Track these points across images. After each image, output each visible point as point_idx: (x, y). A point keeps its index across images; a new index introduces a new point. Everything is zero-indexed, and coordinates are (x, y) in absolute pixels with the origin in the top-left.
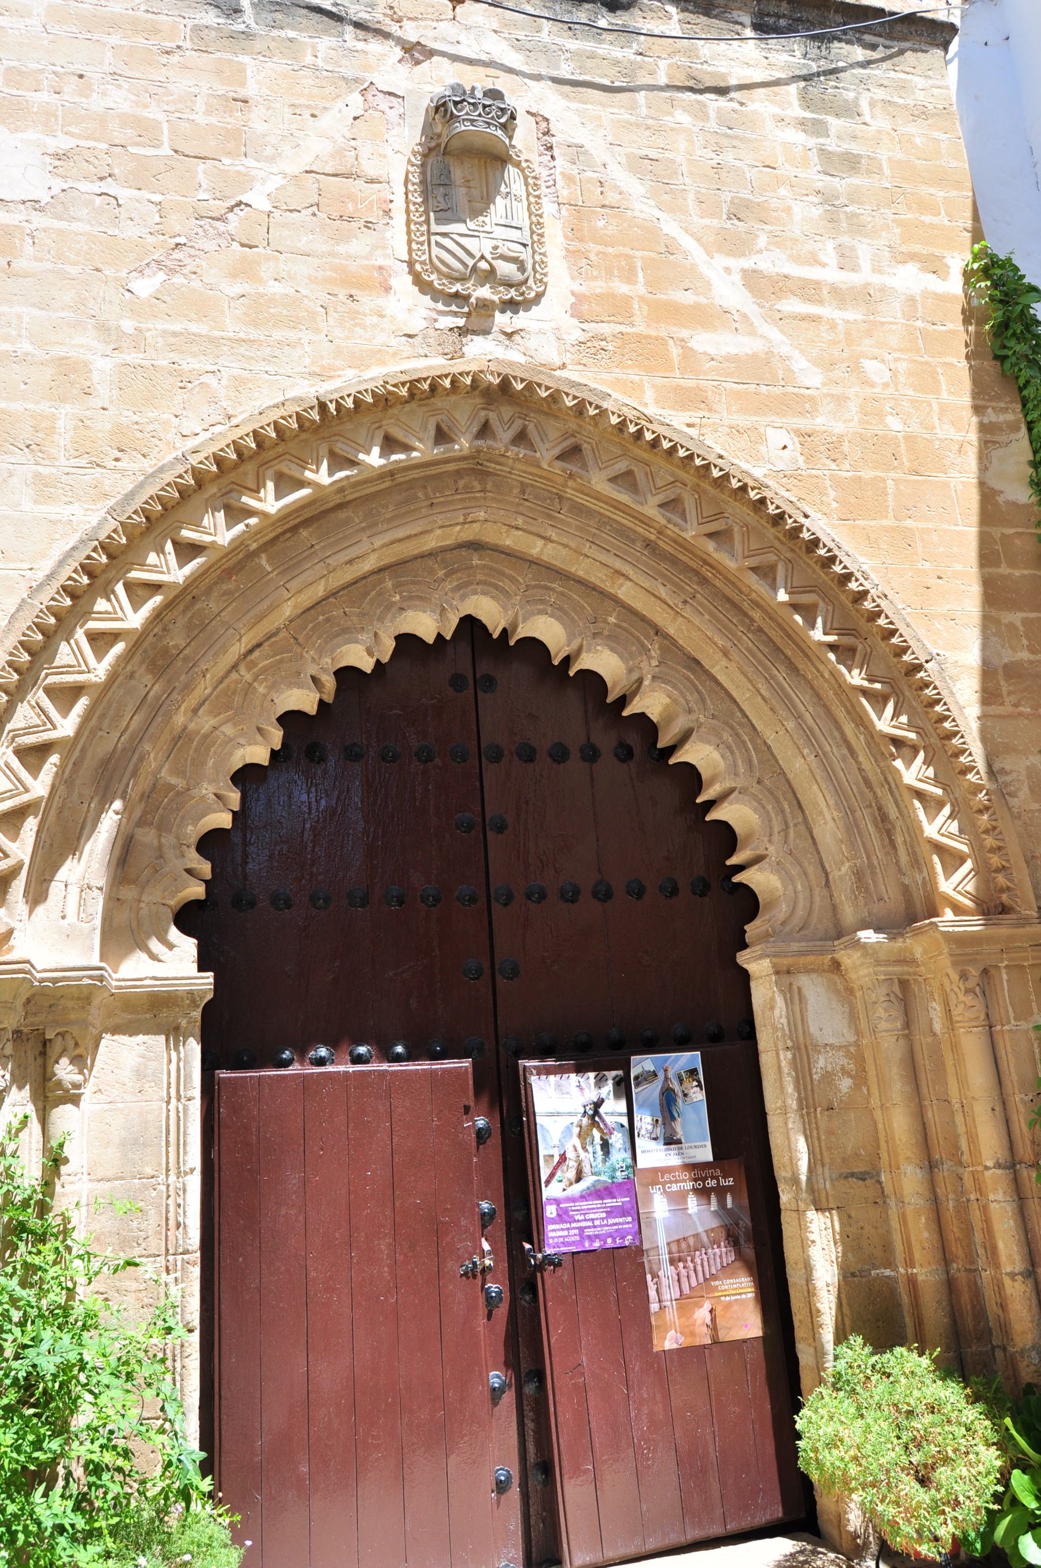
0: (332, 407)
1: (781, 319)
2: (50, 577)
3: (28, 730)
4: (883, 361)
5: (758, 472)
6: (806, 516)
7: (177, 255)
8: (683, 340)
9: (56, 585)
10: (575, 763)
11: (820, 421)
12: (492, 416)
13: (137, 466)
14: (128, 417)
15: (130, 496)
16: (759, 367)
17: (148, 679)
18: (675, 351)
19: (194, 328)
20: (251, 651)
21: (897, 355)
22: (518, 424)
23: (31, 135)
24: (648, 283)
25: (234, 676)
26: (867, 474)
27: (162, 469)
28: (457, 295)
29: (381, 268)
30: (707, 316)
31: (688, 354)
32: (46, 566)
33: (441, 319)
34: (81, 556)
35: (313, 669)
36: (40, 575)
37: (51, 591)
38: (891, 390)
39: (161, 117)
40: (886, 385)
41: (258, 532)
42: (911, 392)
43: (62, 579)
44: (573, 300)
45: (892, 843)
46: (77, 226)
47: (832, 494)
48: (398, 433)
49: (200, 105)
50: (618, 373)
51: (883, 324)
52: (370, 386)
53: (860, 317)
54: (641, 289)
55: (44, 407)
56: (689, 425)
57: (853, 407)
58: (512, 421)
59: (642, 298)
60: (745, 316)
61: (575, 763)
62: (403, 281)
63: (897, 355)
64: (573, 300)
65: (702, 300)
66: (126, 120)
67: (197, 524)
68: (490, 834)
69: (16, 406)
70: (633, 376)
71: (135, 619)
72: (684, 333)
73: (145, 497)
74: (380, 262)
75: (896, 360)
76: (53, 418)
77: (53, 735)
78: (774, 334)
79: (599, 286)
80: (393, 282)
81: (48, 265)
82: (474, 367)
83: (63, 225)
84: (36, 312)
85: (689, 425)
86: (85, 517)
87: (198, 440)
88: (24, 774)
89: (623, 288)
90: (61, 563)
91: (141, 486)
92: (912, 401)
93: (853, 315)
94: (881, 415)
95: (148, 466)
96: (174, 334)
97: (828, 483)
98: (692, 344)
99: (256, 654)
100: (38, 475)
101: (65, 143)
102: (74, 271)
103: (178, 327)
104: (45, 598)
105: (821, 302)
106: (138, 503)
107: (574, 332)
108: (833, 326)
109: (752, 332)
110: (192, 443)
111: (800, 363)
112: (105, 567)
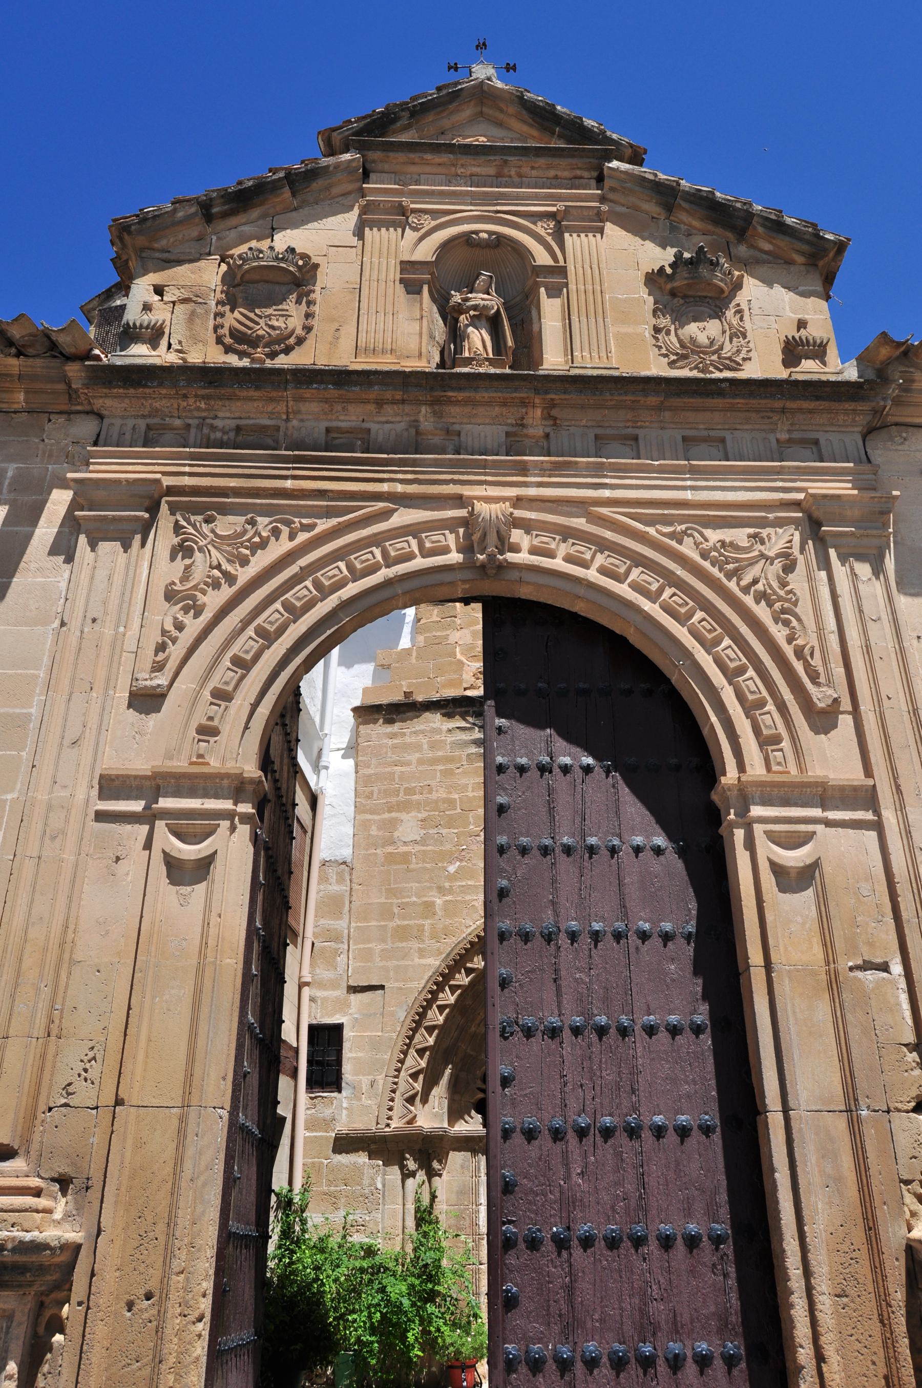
2: (424, 988)
3: (420, 1043)
7: (463, 853)
9: (426, 990)
13: (451, 941)
14: (448, 921)
15: (448, 955)
19: (469, 883)
23: (413, 814)
27: (459, 943)
34: (433, 979)
36: (422, 985)
37: (424, 993)
39: (456, 796)
43: (428, 988)
46: (429, 848)
49: (470, 789)
55: (421, 922)
66: (445, 801)
67: (472, 961)
69: (411, 922)
71: (452, 999)
76: (424, 925)
77: (427, 1044)
81: (420, 865)
83: (424, 848)
84: (417, 885)
86: (434, 963)
87: (472, 928)
88: (419, 1059)
91: (452, 950)
95: (455, 940)
96: (463, 886)
100: (419, 948)
101: (423, 815)
102: (428, 866)
103: (464, 883)
104: (422, 997)
106: (451, 957)
110: (469, 930)
112: (443, 981)
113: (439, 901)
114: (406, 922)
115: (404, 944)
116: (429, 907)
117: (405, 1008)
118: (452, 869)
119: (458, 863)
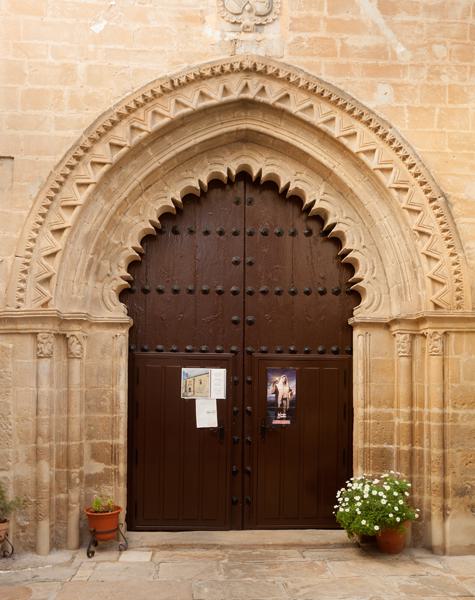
0: (176, 83)
1: (390, 25)
2: (61, 162)
3: (56, 223)
4: (445, 45)
5: (371, 106)
6: (391, 127)
8: (342, 40)
9: (64, 165)
10: (287, 238)
11: (407, 79)
12: (249, 82)
15: (91, 126)
16: (380, 52)
17: (103, 201)
18: (339, 45)
19: (119, 47)
20: (147, 188)
21: (455, 40)
22: (261, 85)
24: (328, 10)
25: (140, 199)
26: (427, 105)
28: (235, 23)
29: (201, 11)
30: (356, 27)
31: (344, 48)
32: (60, 157)
33: (228, 34)
35: (172, 195)
36: (58, 161)
38: (447, 60)
40: (444, 59)
41: (146, 139)
42: (457, 61)
44: (291, 21)
45: (416, 277)
47: (407, 115)
48: (205, 91)
50: (310, 59)
51: (449, 23)
52: (192, 71)
53: (436, 21)
54: (325, 13)
56: (340, 84)
57: (424, 73)
58: (258, 84)
59: (325, 19)
60: (375, 25)
61: (287, 238)
62: (211, 18)
63: (455, 40)
64: (291, 21)
65: (355, 18)
68: (246, 266)
69: (48, 87)
70: (316, 60)
72: (345, 36)
73: (97, 126)
74: (201, 8)
75: (453, 43)
78: (388, 33)
79: (304, 13)
80: (207, 18)
82: (240, 60)
85: (340, 84)
89: (315, 13)
90: (66, 156)
92: (457, 66)
93: (434, 19)
94: (438, 74)
95: (100, 112)
97: (406, 110)
98: (347, 42)
99: (149, 190)
100: (56, 118)
103: (112, 47)
105: (416, 14)
107: (292, 37)
108: (421, 26)
109: (378, 33)
111: (400, 49)
113: (81, 67)
114: (39, 87)
115: (38, 112)
116: (68, 72)
117: (39, 184)
118: (98, 28)
119: (105, 22)
